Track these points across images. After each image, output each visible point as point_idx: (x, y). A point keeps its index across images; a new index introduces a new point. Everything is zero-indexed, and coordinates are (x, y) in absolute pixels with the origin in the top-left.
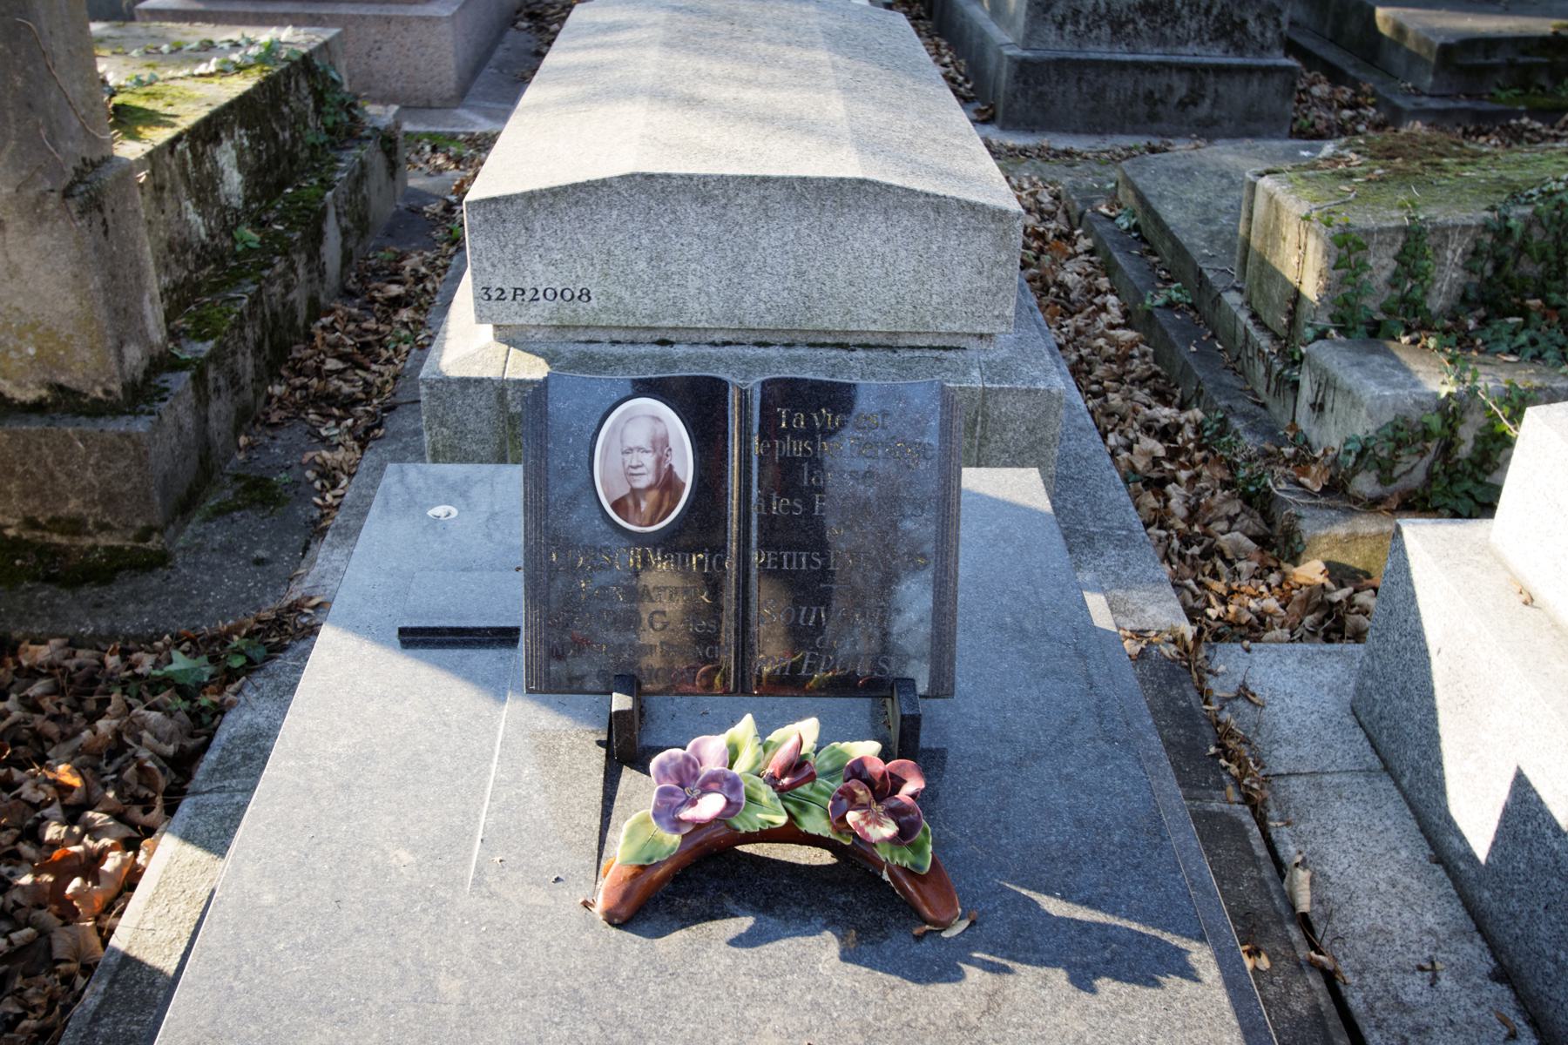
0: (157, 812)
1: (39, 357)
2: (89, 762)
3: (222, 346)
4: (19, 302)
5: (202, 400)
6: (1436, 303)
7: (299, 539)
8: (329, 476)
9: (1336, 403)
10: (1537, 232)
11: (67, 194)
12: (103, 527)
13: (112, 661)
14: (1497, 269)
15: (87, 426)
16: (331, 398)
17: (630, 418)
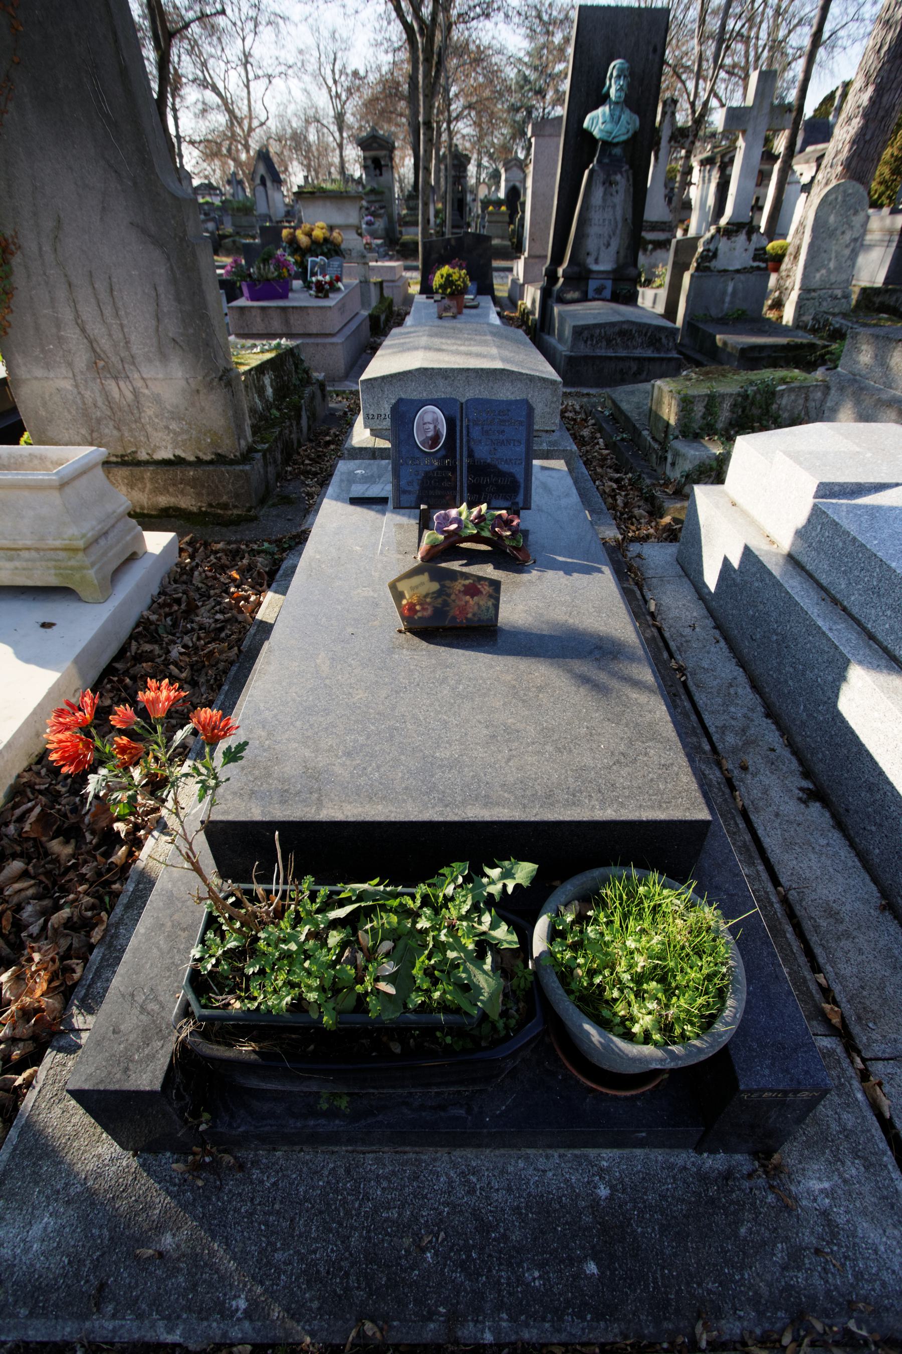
0: (265, 586)
1: (212, 443)
2: (240, 571)
3: (270, 447)
4: (204, 422)
5: (266, 465)
6: (720, 425)
7: (302, 514)
8: (310, 495)
9: (680, 461)
10: (758, 397)
11: (221, 379)
12: (235, 507)
13: (243, 547)
14: (743, 411)
15: (229, 468)
16: (308, 472)
17: (425, 412)
